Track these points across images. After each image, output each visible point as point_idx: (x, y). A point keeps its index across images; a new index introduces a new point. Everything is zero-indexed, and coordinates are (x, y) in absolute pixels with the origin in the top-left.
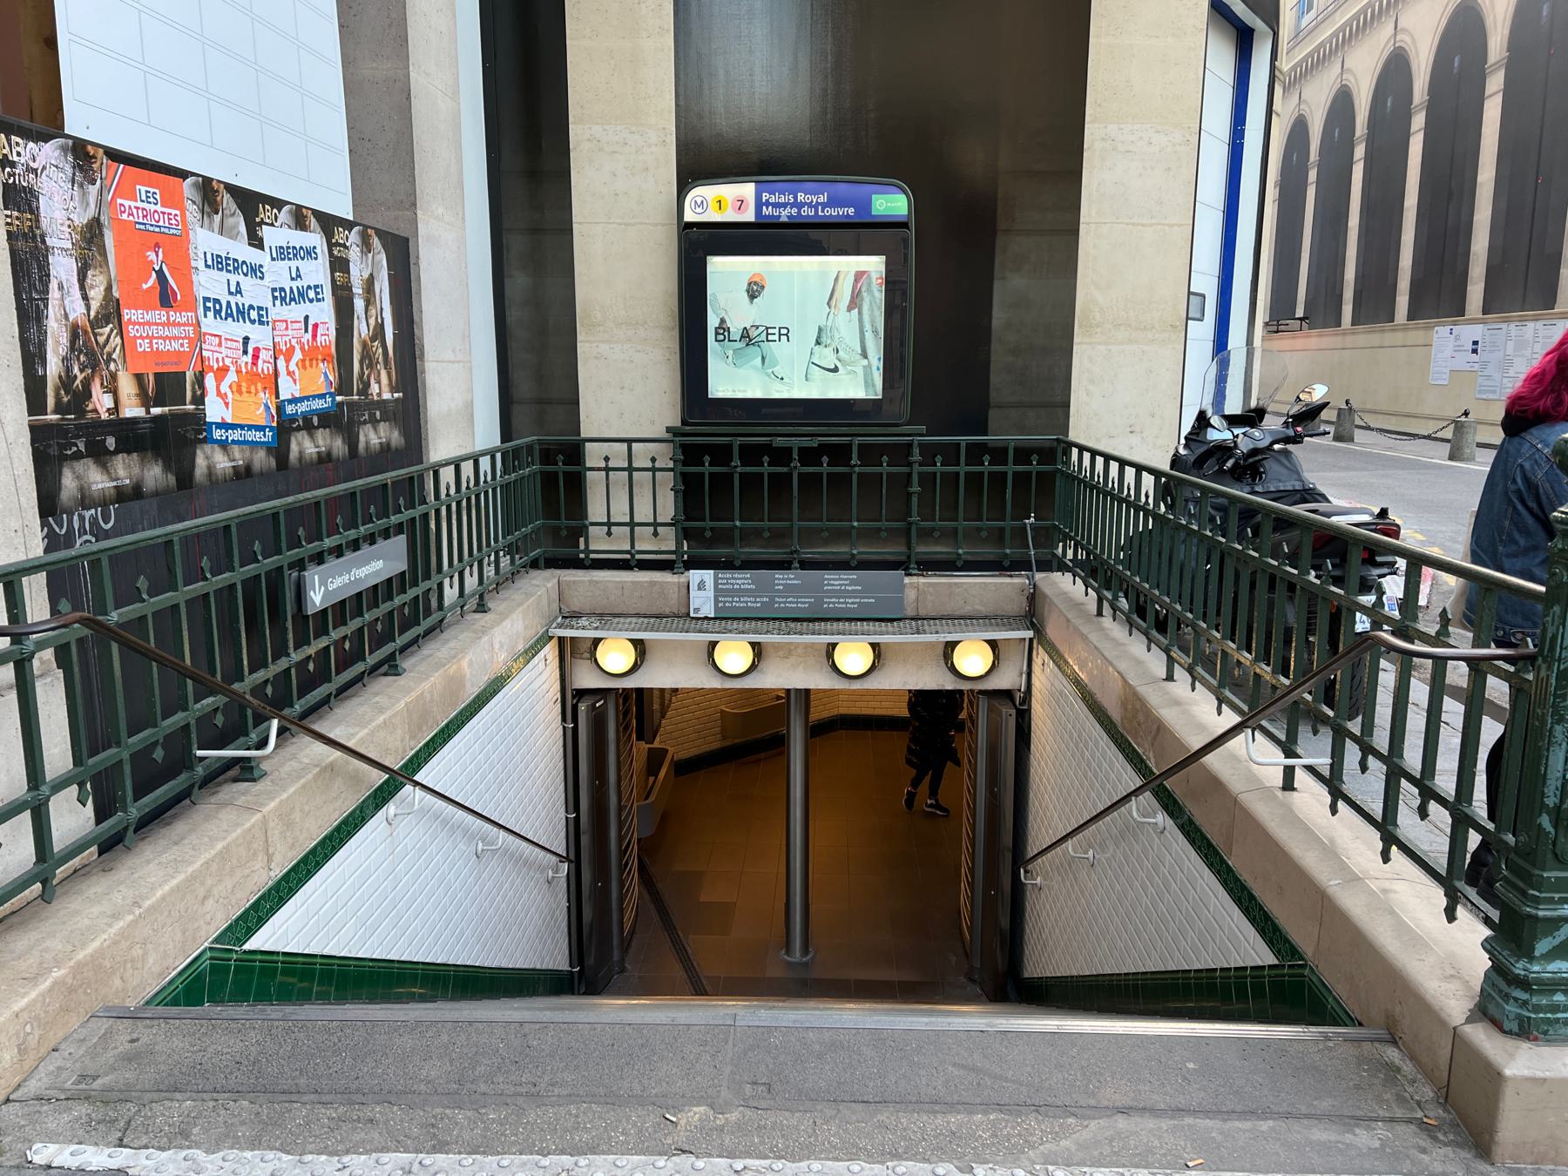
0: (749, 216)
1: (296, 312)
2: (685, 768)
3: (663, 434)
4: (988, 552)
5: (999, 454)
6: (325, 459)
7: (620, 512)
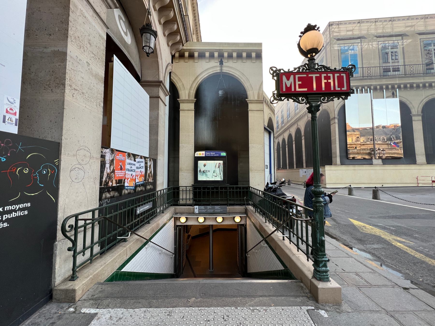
0: (204, 156)
1: (139, 170)
2: (194, 238)
3: (191, 185)
4: (239, 203)
5: (240, 188)
6: (141, 191)
7: (184, 197)
